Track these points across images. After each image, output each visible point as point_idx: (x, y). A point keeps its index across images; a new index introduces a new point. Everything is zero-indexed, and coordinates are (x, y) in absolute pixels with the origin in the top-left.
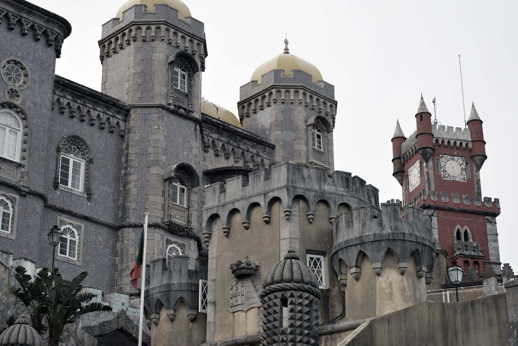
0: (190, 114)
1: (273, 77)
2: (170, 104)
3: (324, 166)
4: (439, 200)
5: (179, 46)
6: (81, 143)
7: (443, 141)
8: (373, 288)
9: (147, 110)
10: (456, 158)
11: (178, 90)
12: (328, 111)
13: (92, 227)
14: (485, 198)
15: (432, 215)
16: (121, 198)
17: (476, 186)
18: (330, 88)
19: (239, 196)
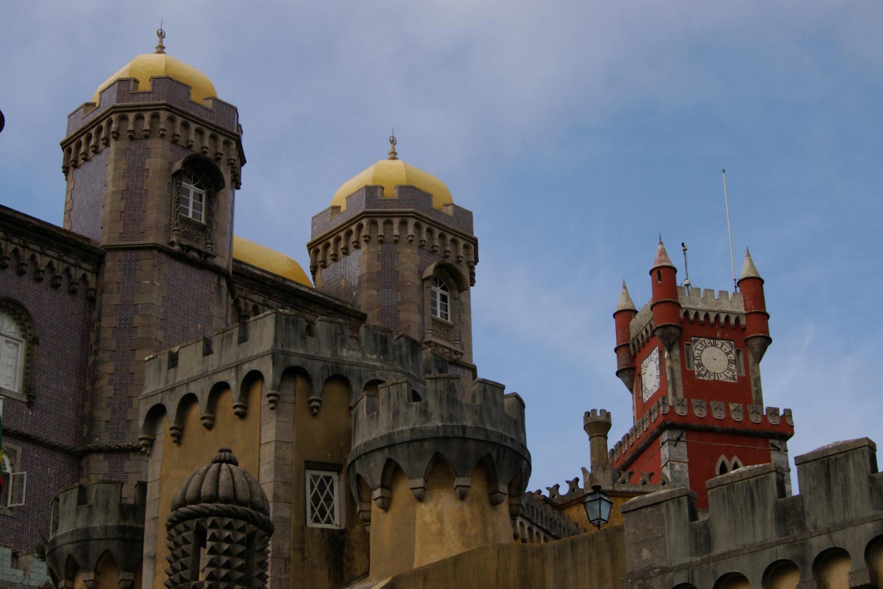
0: (209, 259)
1: (364, 198)
2: (172, 244)
3: (453, 347)
4: (691, 413)
5: (192, 146)
6: (18, 311)
7: (697, 315)
8: (410, 524)
9: (134, 254)
10: (719, 343)
11: (189, 219)
12: (461, 254)
13: (36, 453)
14: (768, 409)
15: (678, 440)
16: (87, 404)
17: (754, 389)
18: (465, 216)
19: (196, 371)
